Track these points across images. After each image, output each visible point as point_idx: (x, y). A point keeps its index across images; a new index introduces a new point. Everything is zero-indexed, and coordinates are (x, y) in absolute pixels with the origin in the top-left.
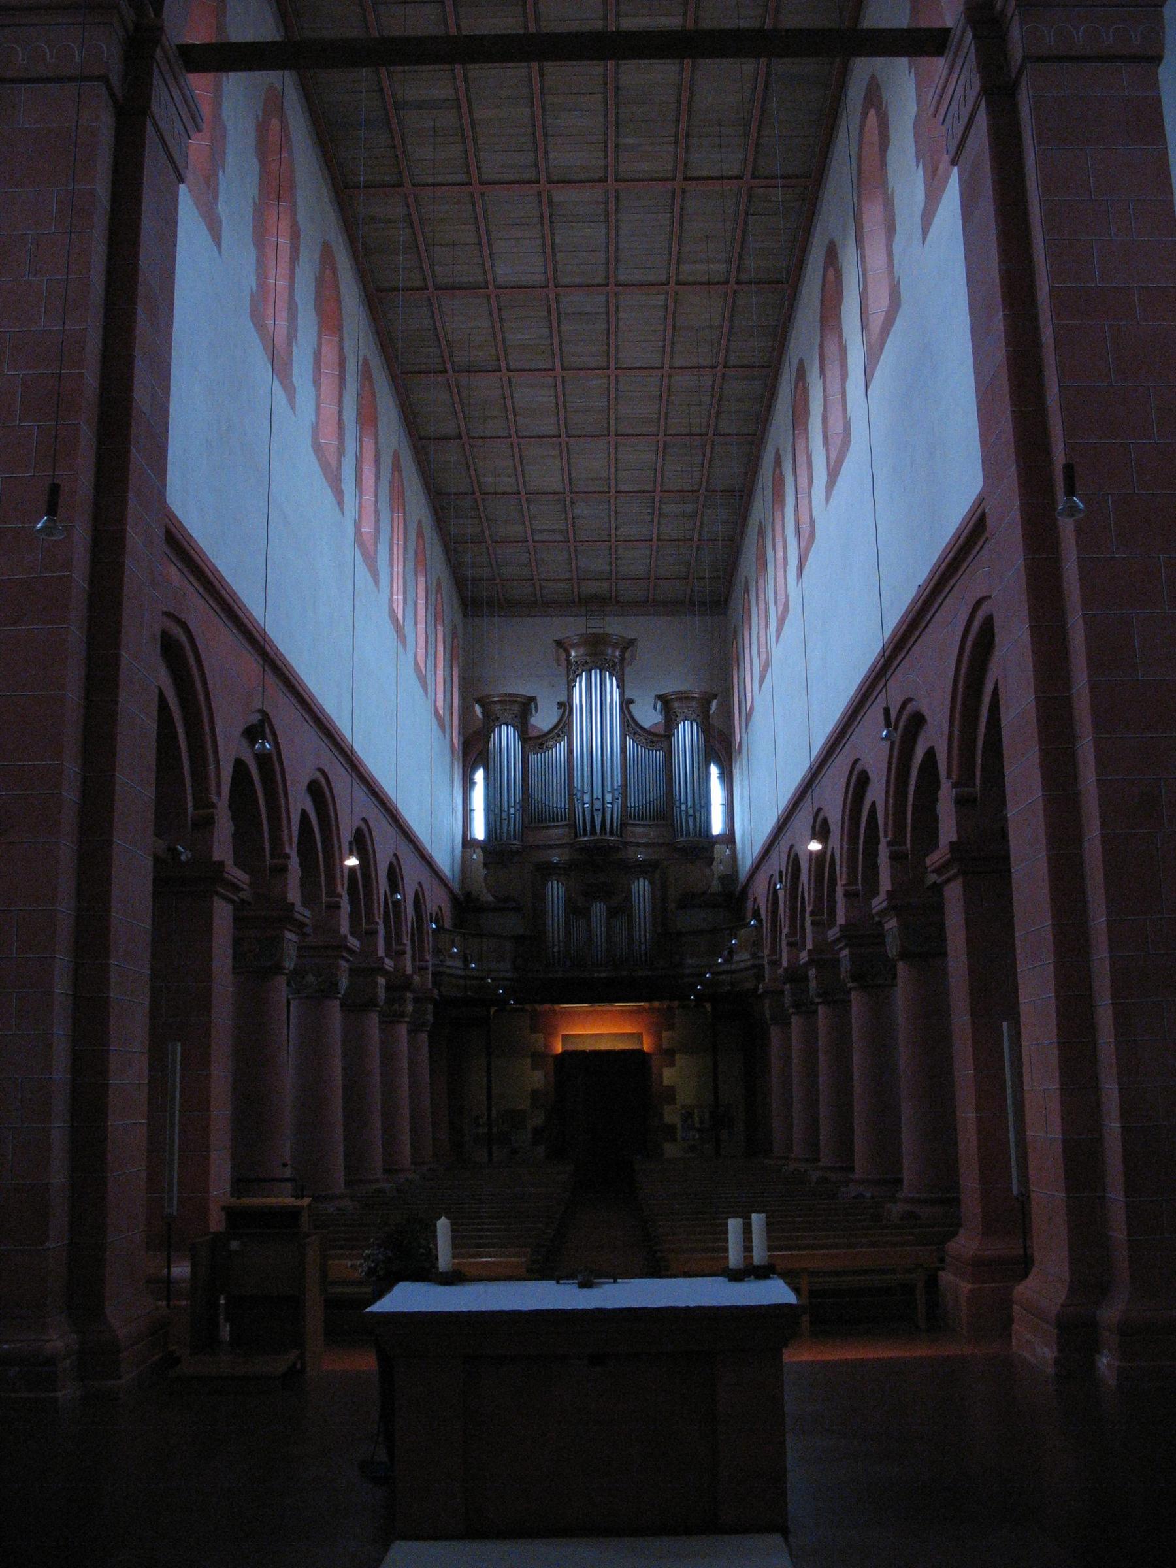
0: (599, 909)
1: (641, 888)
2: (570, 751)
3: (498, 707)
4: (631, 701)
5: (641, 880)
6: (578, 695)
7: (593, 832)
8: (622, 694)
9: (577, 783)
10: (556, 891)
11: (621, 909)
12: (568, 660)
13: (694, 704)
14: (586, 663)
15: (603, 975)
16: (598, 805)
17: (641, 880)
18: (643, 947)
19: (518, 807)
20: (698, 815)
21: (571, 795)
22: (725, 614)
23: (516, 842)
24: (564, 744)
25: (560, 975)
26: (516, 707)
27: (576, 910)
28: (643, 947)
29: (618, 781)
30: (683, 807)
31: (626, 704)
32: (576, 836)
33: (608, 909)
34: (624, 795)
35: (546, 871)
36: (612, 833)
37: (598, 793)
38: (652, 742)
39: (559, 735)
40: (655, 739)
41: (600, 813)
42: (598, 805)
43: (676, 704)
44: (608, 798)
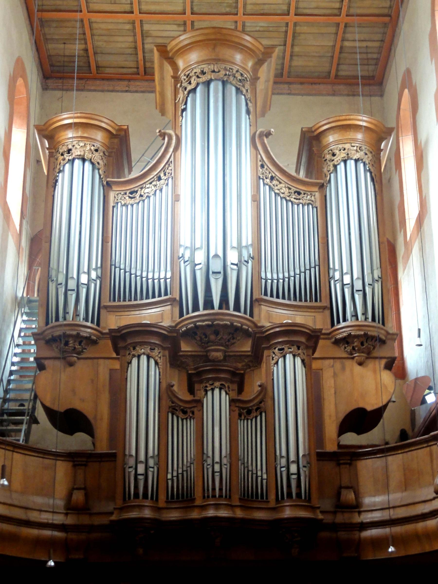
0: (217, 403)
1: (288, 373)
2: (176, 198)
3: (70, 134)
4: (268, 134)
5: (289, 357)
6: (190, 125)
7: (209, 304)
8: (253, 124)
9: (185, 239)
10: (145, 375)
11: (252, 408)
12: (176, 78)
13: (359, 136)
14: (203, 73)
15: (223, 513)
16: (216, 266)
17: (289, 357)
18: (293, 468)
19: (94, 275)
20: (368, 290)
21: (175, 259)
22: (382, 96)
23: (89, 324)
24: (168, 191)
25: (147, 513)
26: (99, 136)
27: (180, 407)
28: (293, 468)
29: (248, 238)
30: (347, 279)
31: (259, 139)
32: (181, 315)
33: (232, 401)
34: (257, 258)
35: (126, 341)
36: (237, 307)
37: (216, 247)
38: (299, 193)
39: (159, 179)
40: (301, 188)
41: (221, 277)
42: (216, 266)
43: (331, 138)
44: (233, 257)
